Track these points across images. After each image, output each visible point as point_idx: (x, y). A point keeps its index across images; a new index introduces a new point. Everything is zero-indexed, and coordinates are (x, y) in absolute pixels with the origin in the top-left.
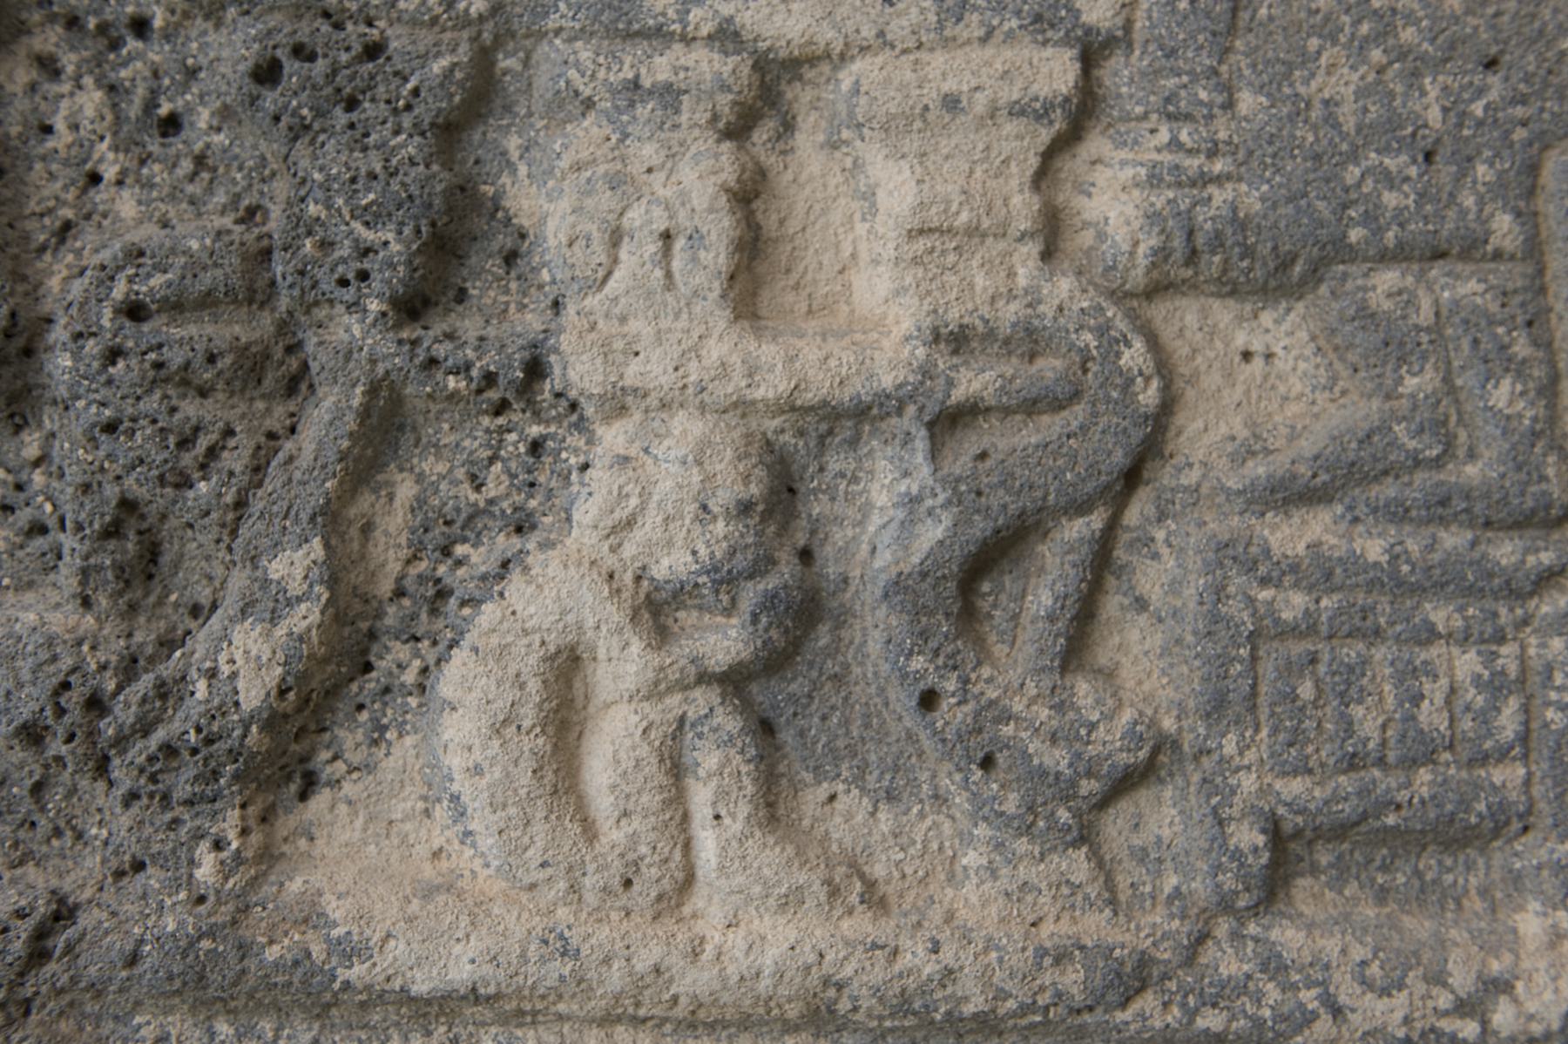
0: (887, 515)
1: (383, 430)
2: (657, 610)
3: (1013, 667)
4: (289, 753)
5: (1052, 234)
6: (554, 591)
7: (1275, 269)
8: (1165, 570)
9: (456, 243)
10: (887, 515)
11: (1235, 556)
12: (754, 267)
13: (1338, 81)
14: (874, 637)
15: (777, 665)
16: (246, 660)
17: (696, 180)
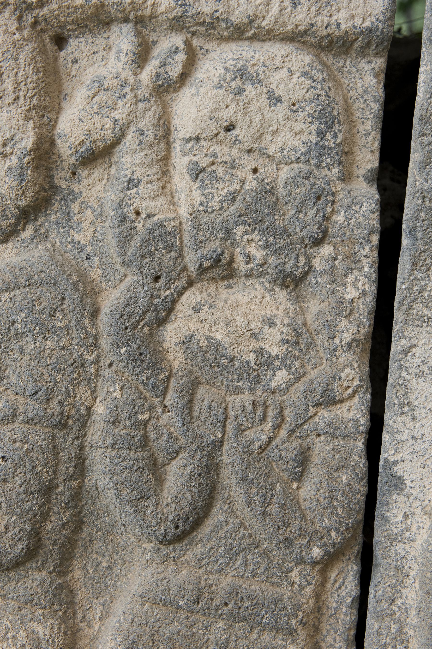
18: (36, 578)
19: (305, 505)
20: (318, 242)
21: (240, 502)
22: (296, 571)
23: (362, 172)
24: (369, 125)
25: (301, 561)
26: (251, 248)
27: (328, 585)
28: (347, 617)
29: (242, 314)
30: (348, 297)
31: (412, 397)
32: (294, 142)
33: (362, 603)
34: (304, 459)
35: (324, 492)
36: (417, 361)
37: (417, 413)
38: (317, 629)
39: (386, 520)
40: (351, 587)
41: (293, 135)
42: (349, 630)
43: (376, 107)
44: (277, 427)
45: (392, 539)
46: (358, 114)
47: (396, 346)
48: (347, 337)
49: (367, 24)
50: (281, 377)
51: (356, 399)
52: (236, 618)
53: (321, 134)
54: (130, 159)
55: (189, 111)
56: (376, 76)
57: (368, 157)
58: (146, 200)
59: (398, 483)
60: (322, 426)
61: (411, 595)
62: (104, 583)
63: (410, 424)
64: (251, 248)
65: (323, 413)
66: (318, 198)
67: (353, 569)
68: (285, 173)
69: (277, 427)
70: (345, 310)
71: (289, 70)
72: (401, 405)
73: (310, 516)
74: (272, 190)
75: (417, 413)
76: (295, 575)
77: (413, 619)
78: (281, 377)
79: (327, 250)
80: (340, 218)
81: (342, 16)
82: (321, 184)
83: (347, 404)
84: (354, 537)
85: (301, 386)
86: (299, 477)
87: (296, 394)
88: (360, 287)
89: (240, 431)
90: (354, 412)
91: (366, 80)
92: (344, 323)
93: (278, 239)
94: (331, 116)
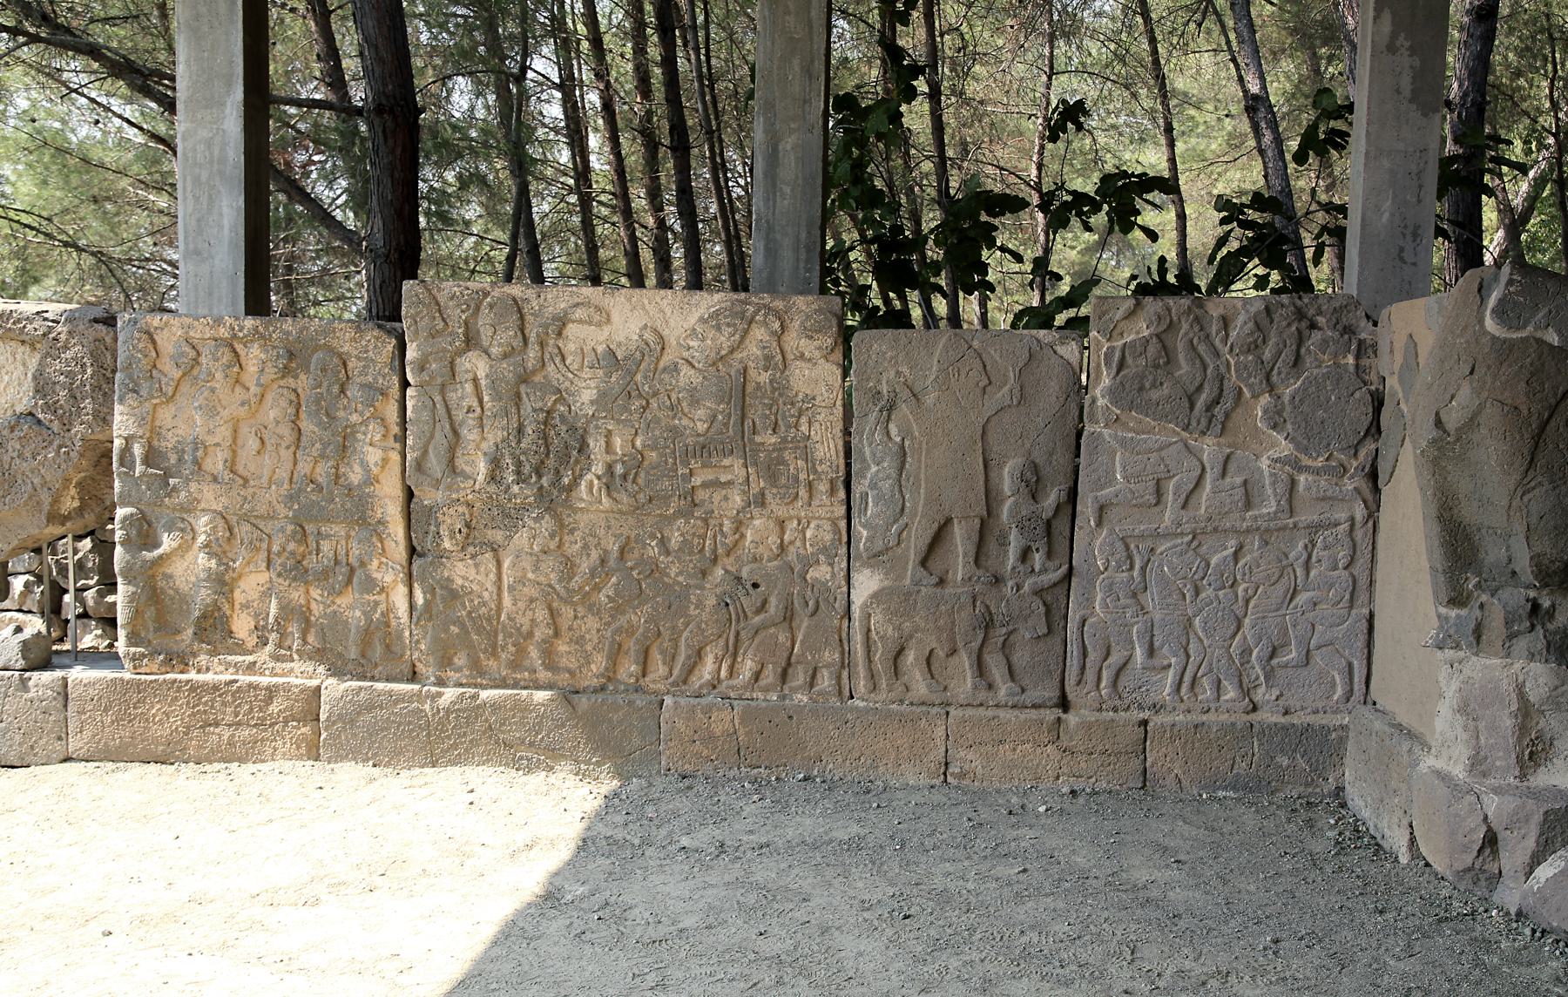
0: (619, 469)
1: (577, 462)
2: (599, 478)
3: (629, 485)
4: (570, 488)
5: (633, 446)
6: (589, 476)
7: (654, 448)
8: (642, 475)
9: (583, 447)
10: (619, 469)
11: (648, 473)
12: (609, 448)
13: (657, 433)
14: (618, 481)
15: (610, 481)
16: (566, 481)
17: (602, 442)
18: (786, 624)
26: (822, 558)
29: (820, 573)
35: (840, 605)
41: (828, 537)
54: (798, 543)
55: (809, 534)
57: (845, 539)
58: (802, 551)
62: (799, 627)
64: (822, 558)
71: (827, 526)
88: (844, 565)
90: (845, 589)
91: (843, 524)
93: (828, 557)
94: (837, 531)
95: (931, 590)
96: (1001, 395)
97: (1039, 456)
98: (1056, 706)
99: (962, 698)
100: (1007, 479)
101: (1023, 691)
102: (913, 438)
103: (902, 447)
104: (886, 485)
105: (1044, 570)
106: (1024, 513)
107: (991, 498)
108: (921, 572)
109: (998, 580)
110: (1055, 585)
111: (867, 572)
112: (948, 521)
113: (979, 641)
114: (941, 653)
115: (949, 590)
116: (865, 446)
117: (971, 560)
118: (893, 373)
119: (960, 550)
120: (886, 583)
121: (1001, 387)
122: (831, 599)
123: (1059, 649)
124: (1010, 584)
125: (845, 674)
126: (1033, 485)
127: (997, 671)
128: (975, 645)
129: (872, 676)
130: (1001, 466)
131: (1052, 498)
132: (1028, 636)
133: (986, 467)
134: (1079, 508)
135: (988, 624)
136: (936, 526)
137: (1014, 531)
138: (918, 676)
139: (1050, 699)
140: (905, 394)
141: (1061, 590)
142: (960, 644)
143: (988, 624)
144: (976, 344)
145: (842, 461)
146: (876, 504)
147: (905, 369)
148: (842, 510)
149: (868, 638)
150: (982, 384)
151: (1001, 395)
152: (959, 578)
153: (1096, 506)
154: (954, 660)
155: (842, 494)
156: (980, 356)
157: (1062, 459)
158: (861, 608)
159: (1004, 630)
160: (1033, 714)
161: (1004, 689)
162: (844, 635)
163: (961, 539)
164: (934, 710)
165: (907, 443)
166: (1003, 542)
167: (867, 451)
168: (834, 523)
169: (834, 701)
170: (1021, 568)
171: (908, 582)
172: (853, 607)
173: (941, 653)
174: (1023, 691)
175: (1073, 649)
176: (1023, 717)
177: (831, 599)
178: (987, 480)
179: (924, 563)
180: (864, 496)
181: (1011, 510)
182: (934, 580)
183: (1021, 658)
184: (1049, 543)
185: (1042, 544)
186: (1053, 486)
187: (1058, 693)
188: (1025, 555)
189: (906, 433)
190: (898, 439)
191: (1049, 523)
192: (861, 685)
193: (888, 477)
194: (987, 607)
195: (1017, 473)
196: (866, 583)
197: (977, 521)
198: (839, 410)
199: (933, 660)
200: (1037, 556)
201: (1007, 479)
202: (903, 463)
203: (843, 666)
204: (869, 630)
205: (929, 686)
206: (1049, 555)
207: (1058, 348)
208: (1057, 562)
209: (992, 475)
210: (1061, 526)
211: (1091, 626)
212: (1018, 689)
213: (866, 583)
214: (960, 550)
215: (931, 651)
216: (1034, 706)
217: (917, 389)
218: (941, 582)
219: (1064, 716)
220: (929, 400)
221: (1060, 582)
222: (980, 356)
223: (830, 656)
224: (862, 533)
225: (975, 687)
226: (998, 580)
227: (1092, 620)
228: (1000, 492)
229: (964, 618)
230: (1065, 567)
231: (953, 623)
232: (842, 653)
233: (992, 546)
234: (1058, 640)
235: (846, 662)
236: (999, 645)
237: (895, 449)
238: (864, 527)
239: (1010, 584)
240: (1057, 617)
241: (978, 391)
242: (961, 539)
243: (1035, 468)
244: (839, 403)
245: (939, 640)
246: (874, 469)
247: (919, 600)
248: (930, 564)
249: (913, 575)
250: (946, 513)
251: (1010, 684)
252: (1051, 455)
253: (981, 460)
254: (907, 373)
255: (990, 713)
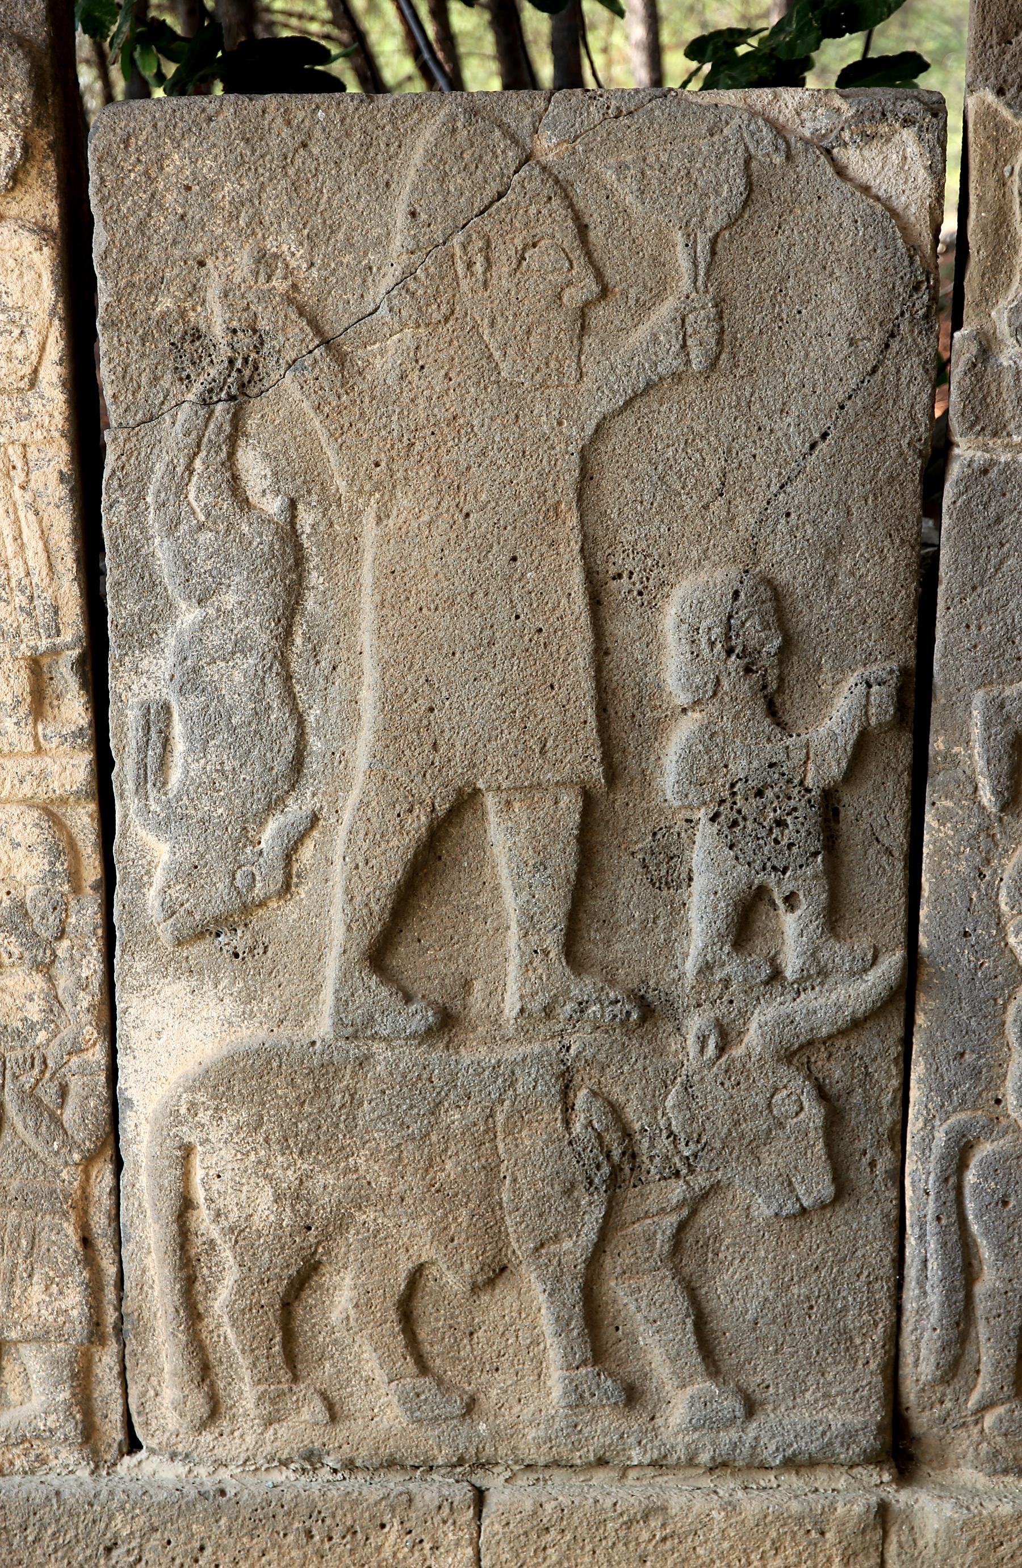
19: (66, 1126)
20: (59, 939)
21: (20, 1127)
22: (65, 1172)
23: (89, 883)
24: (89, 850)
25: (66, 1164)
27: (92, 1181)
28: (107, 1202)
30: (84, 975)
31: (132, 1042)
32: (32, 872)
33: (116, 1190)
34: (63, 1092)
35: (79, 1114)
36: (133, 1018)
37: (136, 1053)
38: (86, 1212)
39: (125, 1130)
40: (108, 1179)
42: (109, 1211)
43: (93, 837)
44: (42, 1072)
45: (129, 1143)
46: (80, 844)
47: (120, 1007)
48: (85, 1004)
49: (75, 788)
50: (42, 1037)
51: (98, 1047)
52: (26, 1206)
53: (52, 864)
56: (90, 816)
57: (92, 871)
59: (129, 1102)
60: (74, 1068)
61: (143, 1180)
63: (132, 1061)
65: (75, 1060)
66: (55, 909)
67: (108, 1168)
68: (30, 892)
69: (42, 1072)
70: (83, 985)
72: (125, 1049)
73: (70, 1132)
74: (23, 905)
75: (136, 1053)
76: (64, 1175)
77: (146, 1197)
78: (42, 1037)
79: (66, 943)
80: (73, 920)
81: (56, 785)
82: (57, 897)
83: (91, 1051)
84: (104, 1144)
85: (56, 1041)
86: (62, 1106)
87: (54, 1048)
88: (92, 966)
89: (16, 1077)
90: (97, 1055)
91: (83, 819)
92: (82, 994)
94: (64, 847)
95: (410, 1055)
96: (645, 336)
97: (790, 565)
98: (873, 1459)
99: (530, 1443)
100: (674, 645)
101: (751, 1407)
102: (328, 501)
103: (289, 533)
104: (235, 678)
105: (816, 973)
106: (739, 768)
107: (617, 720)
108: (374, 992)
109: (649, 1011)
110: (856, 1024)
111: (175, 990)
112: (465, 802)
113: (589, 1233)
114: (451, 1280)
115: (473, 1053)
116: (155, 526)
117: (552, 942)
118: (243, 259)
119: (511, 903)
120: (251, 1034)
121: (644, 308)
122: (48, 1094)
123: (876, 1253)
124: (695, 1023)
125: (106, 1360)
126: (768, 659)
127: (657, 1344)
128: (574, 1248)
129: (203, 1368)
130: (649, 598)
131: (839, 709)
132: (762, 1210)
133: (596, 600)
134: (937, 744)
135: (617, 1168)
136: (418, 822)
137: (705, 834)
138: (370, 1363)
139: (850, 1436)
140: (293, 337)
141: (878, 1045)
142: (519, 1246)
143: (617, 1168)
144: (547, 145)
145: (69, 594)
146: (200, 745)
147: (287, 245)
148: (76, 769)
149: (184, 1234)
150: (573, 297)
151: (645, 336)
152: (511, 1005)
153: (1002, 734)
154: (502, 1303)
155: (73, 709)
156: (563, 189)
157: (876, 572)
158: (160, 1133)
159: (677, 1191)
160: (788, 1494)
161: (681, 1402)
162: (99, 1222)
163: (512, 864)
164: (429, 1492)
165: (306, 519)
166: (667, 876)
167: (162, 554)
168: (51, 814)
169: (68, 1470)
170: (733, 967)
171: (322, 1026)
172: (128, 1122)
173: (451, 1280)
174: (751, 1407)
175: (925, 1250)
176: (751, 1505)
177: (48, 1094)
178: (600, 652)
179: (379, 956)
180: (157, 719)
181: (690, 758)
182: (418, 1017)
183: (740, 1287)
184: (834, 875)
185: (806, 878)
186: (842, 668)
187: (874, 1413)
188: (746, 919)
189: (301, 483)
190: (273, 506)
191: (829, 805)
192: (165, 1399)
193: (241, 646)
194: (615, 1110)
195: (711, 623)
196: (178, 1035)
197: (570, 802)
198: (52, 400)
199: (423, 1304)
200: (790, 923)
201: (674, 645)
202: (294, 594)
203: (95, 1332)
204: (186, 1205)
205: (410, 1401)
206: (834, 917)
207: (851, 157)
208: (863, 944)
209: (622, 629)
210: (875, 811)
211: (993, 1168)
212: (731, 1405)
213: (178, 1035)
214: (511, 903)
215: (416, 1276)
216: (791, 1464)
217: (336, 317)
218: (446, 1023)
219: (901, 1498)
220: (383, 358)
221: (877, 1012)
222: (563, 189)
223: (53, 1300)
224: (150, 848)
225: (577, 1400)
226: (649, 1011)
227: (985, 1149)
228: (649, 694)
229: (532, 1151)
230: (892, 962)
231: (492, 1170)
232: (94, 1289)
233: (625, 887)
234: (872, 1219)
235: (107, 1322)
236: (662, 1242)
237: (264, 540)
238: (162, 826)
239: (695, 1023)
240: (865, 1138)
241: (560, 321)
242: (512, 864)
243: (777, 604)
244: (52, 374)
245: (442, 1235)
246: (188, 615)
247: (367, 1090)
248: (404, 957)
249: (342, 1004)
250: (456, 774)
251: (703, 1385)
252: (831, 554)
253: (576, 578)
254: (298, 261)
255: (632, 1493)
